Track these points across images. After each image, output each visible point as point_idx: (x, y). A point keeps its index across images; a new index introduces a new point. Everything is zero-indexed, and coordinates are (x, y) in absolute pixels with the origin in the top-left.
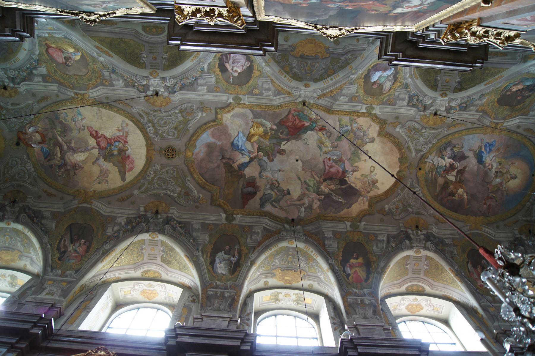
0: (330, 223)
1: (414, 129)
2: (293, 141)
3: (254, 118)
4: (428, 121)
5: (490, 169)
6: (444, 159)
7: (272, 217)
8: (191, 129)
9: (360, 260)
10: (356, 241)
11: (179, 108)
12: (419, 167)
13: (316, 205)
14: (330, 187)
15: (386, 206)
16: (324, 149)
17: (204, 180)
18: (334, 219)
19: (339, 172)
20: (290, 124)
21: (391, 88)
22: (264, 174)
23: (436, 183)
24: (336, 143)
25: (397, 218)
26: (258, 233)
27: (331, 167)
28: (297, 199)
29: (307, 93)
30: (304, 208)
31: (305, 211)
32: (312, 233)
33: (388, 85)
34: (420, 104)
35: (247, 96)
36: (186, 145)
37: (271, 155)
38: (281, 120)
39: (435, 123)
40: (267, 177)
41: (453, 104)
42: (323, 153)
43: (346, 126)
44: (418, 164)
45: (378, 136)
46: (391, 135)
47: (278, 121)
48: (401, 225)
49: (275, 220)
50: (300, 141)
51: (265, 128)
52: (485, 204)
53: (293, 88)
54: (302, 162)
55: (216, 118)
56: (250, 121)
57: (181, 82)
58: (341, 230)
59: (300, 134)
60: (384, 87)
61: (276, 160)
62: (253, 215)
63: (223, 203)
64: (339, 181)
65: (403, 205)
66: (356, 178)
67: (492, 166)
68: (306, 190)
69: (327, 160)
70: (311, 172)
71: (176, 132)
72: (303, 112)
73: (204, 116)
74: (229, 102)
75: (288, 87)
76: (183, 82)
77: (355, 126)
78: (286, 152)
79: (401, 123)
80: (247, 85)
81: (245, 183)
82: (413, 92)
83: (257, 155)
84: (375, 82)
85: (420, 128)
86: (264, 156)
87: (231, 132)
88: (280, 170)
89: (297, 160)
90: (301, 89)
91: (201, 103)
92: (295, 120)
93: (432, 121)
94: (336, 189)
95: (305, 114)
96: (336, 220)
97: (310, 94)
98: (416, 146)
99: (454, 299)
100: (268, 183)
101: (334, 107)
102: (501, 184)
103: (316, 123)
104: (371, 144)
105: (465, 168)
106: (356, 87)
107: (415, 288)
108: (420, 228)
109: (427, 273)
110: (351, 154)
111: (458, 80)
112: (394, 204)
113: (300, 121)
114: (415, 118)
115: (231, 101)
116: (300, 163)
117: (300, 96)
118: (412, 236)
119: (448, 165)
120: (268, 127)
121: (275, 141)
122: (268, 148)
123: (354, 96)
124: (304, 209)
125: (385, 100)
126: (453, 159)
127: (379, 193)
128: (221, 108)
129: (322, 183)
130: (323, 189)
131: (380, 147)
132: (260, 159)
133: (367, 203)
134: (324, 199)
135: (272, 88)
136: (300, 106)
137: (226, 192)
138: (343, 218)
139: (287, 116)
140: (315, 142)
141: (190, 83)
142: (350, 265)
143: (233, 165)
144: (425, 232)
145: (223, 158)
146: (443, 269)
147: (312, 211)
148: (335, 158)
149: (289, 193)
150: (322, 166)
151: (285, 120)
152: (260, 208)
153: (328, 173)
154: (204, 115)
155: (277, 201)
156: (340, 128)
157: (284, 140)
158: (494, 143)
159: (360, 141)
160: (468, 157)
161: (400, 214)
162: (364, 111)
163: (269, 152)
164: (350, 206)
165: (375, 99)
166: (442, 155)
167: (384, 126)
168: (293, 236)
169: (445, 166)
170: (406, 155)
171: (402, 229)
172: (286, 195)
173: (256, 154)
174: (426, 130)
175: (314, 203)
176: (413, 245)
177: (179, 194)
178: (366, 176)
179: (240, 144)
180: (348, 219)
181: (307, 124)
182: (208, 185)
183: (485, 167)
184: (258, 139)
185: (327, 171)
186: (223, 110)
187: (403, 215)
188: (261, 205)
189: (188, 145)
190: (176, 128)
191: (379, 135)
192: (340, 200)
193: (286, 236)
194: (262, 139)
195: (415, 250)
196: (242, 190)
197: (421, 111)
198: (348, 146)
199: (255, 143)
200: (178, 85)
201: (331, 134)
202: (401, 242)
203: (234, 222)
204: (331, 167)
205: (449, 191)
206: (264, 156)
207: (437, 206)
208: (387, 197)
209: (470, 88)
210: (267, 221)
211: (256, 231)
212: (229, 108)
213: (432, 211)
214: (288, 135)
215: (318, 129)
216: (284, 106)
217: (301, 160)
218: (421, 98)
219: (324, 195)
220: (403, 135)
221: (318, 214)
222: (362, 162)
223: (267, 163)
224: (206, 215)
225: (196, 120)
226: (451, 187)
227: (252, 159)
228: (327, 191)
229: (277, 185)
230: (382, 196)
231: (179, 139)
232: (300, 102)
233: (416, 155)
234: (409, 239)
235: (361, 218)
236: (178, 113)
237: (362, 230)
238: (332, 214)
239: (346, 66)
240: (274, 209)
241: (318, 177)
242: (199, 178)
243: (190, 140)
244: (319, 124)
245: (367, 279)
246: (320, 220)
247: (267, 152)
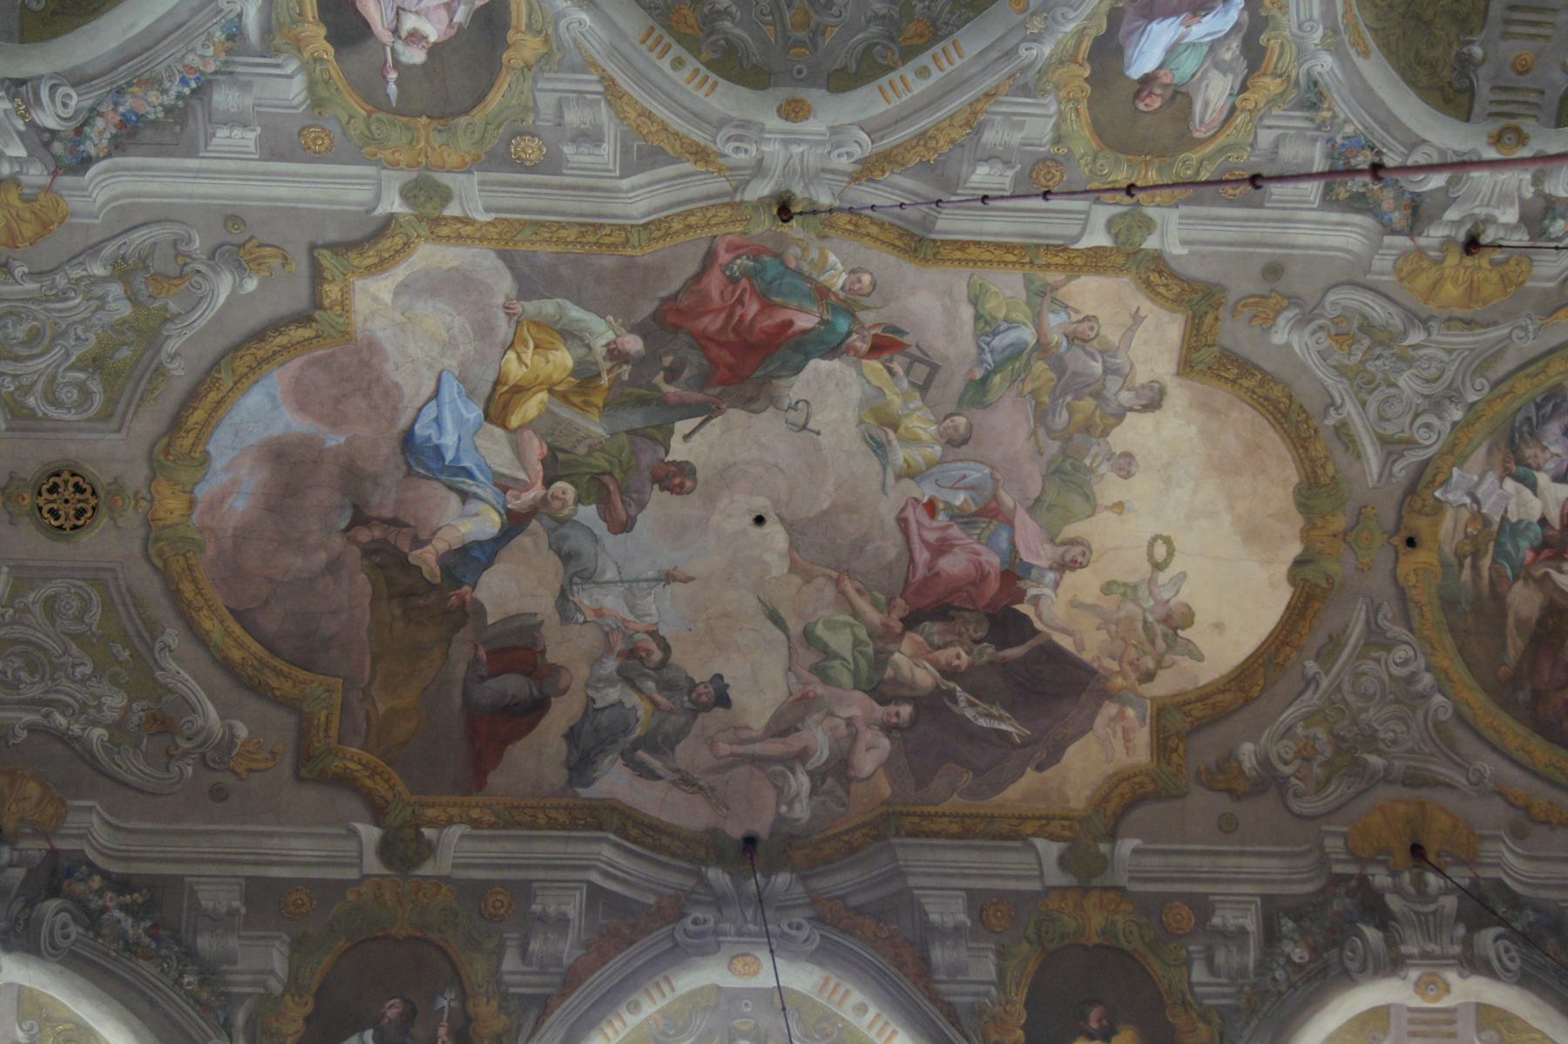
0: (953, 848)
1: (1367, 327)
2: (736, 415)
3: (518, 299)
4: (1436, 285)
7: (634, 832)
8: (176, 368)
10: (1096, 940)
11: (109, 249)
12: (1404, 534)
13: (872, 755)
14: (943, 656)
16: (900, 455)
17: (256, 647)
18: (970, 830)
19: (984, 576)
20: (711, 323)
21: (1233, 110)
22: (585, 598)
24: (961, 421)
26: (563, 920)
27: (941, 548)
28: (768, 727)
29: (796, 150)
30: (811, 774)
31: (814, 792)
32: (858, 910)
34: (1389, 194)
35: (477, 176)
36: (150, 458)
37: (616, 498)
38: (664, 301)
39: (1472, 291)
40: (599, 613)
42: (898, 477)
43: (1012, 324)
44: (1400, 518)
45: (1178, 374)
46: (1246, 367)
47: (647, 308)
48: (1333, 845)
49: (654, 848)
50: (769, 413)
51: (582, 351)
53: (723, 122)
54: (789, 526)
55: (317, 305)
56: (501, 314)
57: (116, 104)
58: (1012, 885)
59: (771, 377)
60: (1198, 107)
61: (644, 520)
62: (533, 826)
63: (365, 766)
64: (986, 625)
65: (1337, 739)
66: (1075, 604)
68: (816, 679)
69: (920, 509)
70: (837, 582)
71: (95, 386)
72: (779, 256)
73: (252, 295)
74: (382, 210)
75: (697, 118)
76: (128, 104)
77: (1055, 321)
78: (700, 476)
79: (1294, 300)
80: (478, 115)
81: (482, 652)
82: (1349, 130)
83: (544, 500)
85: (1398, 322)
86: (579, 500)
87: (399, 377)
88: (668, 578)
89: (760, 520)
90: (762, 129)
91: (233, 219)
92: (740, 301)
93: (1455, 282)
94: (971, 667)
95: (793, 265)
96: (985, 835)
97: (813, 158)
98: (1382, 418)
100: (609, 648)
101: (940, 225)
103: (852, 315)
104: (1146, 421)
106: (1053, 109)
108: (1431, 858)
110: (1044, 478)
112: (1288, 732)
113: (767, 306)
114: (1368, 271)
115: (393, 204)
116: (776, 534)
117: (759, 169)
118: (1394, 903)
120: (599, 345)
121: (636, 419)
122: (600, 461)
123: (1044, 160)
124: (805, 781)
127: (1202, 683)
128: (340, 248)
129: (902, 635)
130: (906, 671)
131: (1192, 431)
132: (562, 522)
133: (1143, 737)
134: (914, 721)
135: (611, 131)
136: (764, 226)
137: (382, 709)
138: (1023, 819)
139: (698, 278)
140: (851, 415)
141: (168, 110)
143: (414, 557)
144: (1462, 876)
145: (360, 518)
147: (853, 787)
148: (959, 499)
149: (723, 700)
150: (892, 547)
151: (684, 302)
152: (571, 783)
153: (925, 581)
154: (251, 285)
155: (660, 742)
156: (977, 336)
157: (688, 410)
159: (1088, 404)
161: (1322, 785)
162: (1098, 238)
163: (606, 479)
164: (1055, 753)
167: (1209, 319)
168: (752, 927)
170: (1330, 470)
171: (1338, 869)
172: (706, 708)
173: (537, 492)
174: (1428, 331)
175: (861, 746)
176: (1404, 949)
177: (117, 727)
178: (1129, 591)
179: (449, 440)
180: (1046, 824)
181: (805, 321)
182: (278, 673)
184: (548, 411)
185: (921, 572)
186: (354, 258)
187: (1337, 791)
188: (570, 769)
189: (167, 452)
190: (96, 363)
191: (1186, 367)
192: (996, 725)
193: (716, 933)
194: (565, 413)
196: (466, 693)
197: (1394, 232)
198: (1023, 432)
199: (528, 434)
200: (100, 123)
201: (934, 368)
202: (1339, 934)
203: (427, 869)
204: (941, 548)
206: (579, 500)
208: (1248, 701)
210: (607, 852)
211: (552, 909)
212: (386, 243)
214: (704, 382)
215: (865, 347)
216: (677, 226)
217: (782, 520)
219: (915, 701)
220: (1313, 361)
221: (885, 803)
222: (1104, 517)
223: (596, 540)
224: (271, 835)
225: (203, 317)
227: (515, 523)
228: (925, 677)
229: (657, 656)
230: (1223, 692)
231: (114, 424)
232: (761, 199)
233: (1383, 466)
234: (1382, 918)
235: (1119, 817)
236: (105, 279)
237: (1123, 880)
238: (956, 803)
240: (643, 785)
241: (874, 603)
242: (228, 633)
243: (176, 424)
244: (867, 317)
246: (897, 834)
247: (596, 478)
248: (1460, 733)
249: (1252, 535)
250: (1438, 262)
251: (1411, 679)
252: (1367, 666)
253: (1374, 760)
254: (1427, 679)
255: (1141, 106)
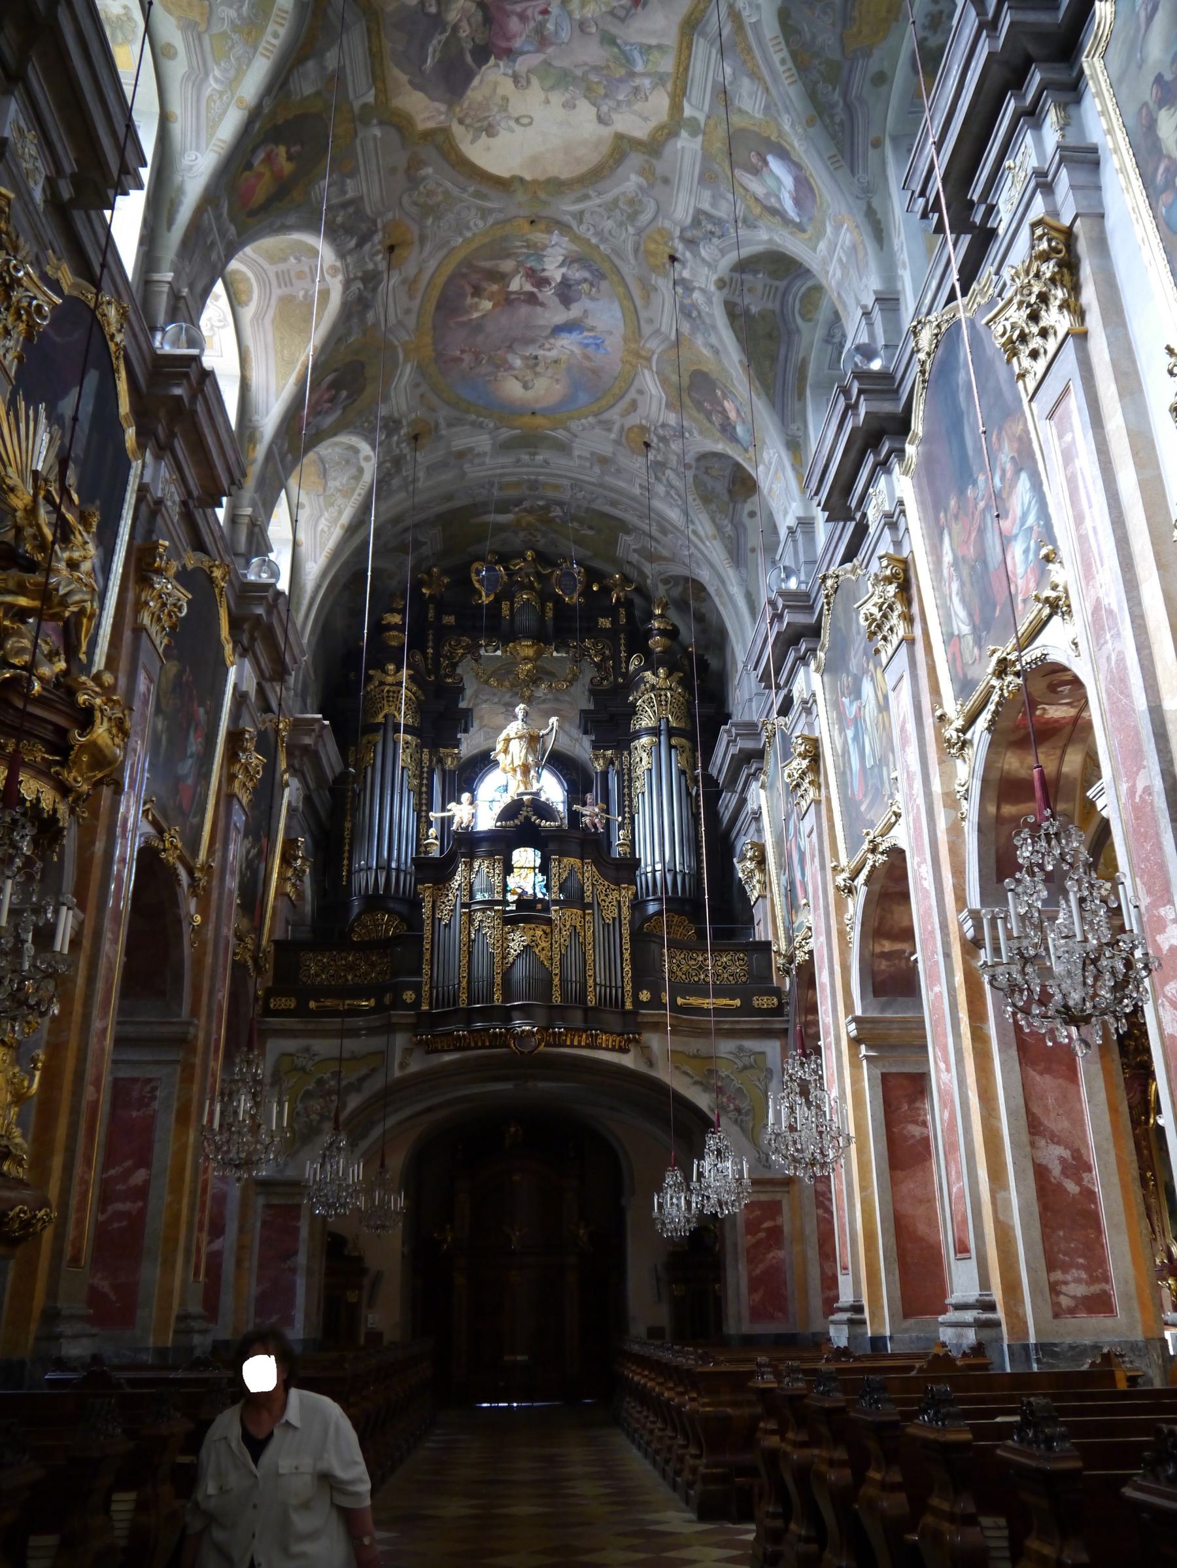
4: (656, 242)
5: (542, 347)
6: (561, 266)
9: (287, 167)
15: (430, 170)
21: (747, 190)
23: (501, 258)
25: (406, 200)
33: (755, 186)
41: (696, 295)
48: (390, 216)
52: (463, 351)
60: (750, 176)
65: (438, 205)
67: (549, 350)
79: (651, 186)
84: (766, 163)
85: (638, 224)
99: (247, 374)
102: (511, 368)
105: (542, 305)
106: (757, 115)
107: (241, 286)
109: (286, 301)
111: (754, 309)
118: (367, 247)
119: (546, 274)
125: (716, 166)
126: (561, 282)
133: (431, 125)
142: (272, 151)
146: (305, 332)
158: (602, 351)
160: (569, 309)
161: (415, 203)
162: (688, 112)
165: (719, 145)
166: (572, 262)
169: (544, 270)
171: (379, 222)
183: (547, 338)
191: (619, 137)
195: (338, 264)
197: (682, 231)
202: (349, 230)
205: (484, 284)
207: (448, 270)
208: (453, 166)
209: (734, 331)
213: (433, 264)
218: (715, 240)
226: (495, 287)
234: (360, 245)
237: (360, 135)
239: (815, 108)
245: (253, 213)
248: (445, 251)
249: (535, 160)
250: (666, 244)
251: (469, 228)
252: (473, 211)
253: (430, 221)
254: (469, 234)
255: (753, 153)
